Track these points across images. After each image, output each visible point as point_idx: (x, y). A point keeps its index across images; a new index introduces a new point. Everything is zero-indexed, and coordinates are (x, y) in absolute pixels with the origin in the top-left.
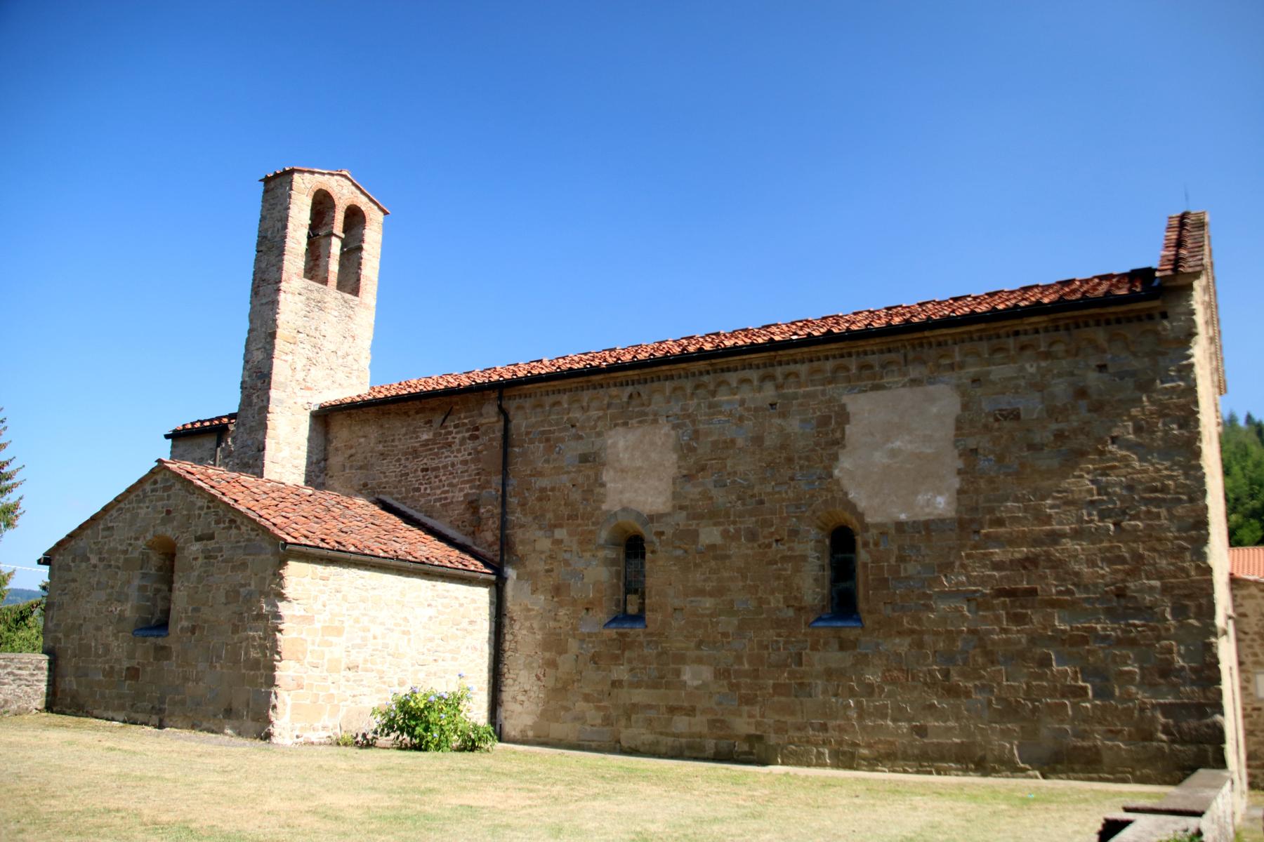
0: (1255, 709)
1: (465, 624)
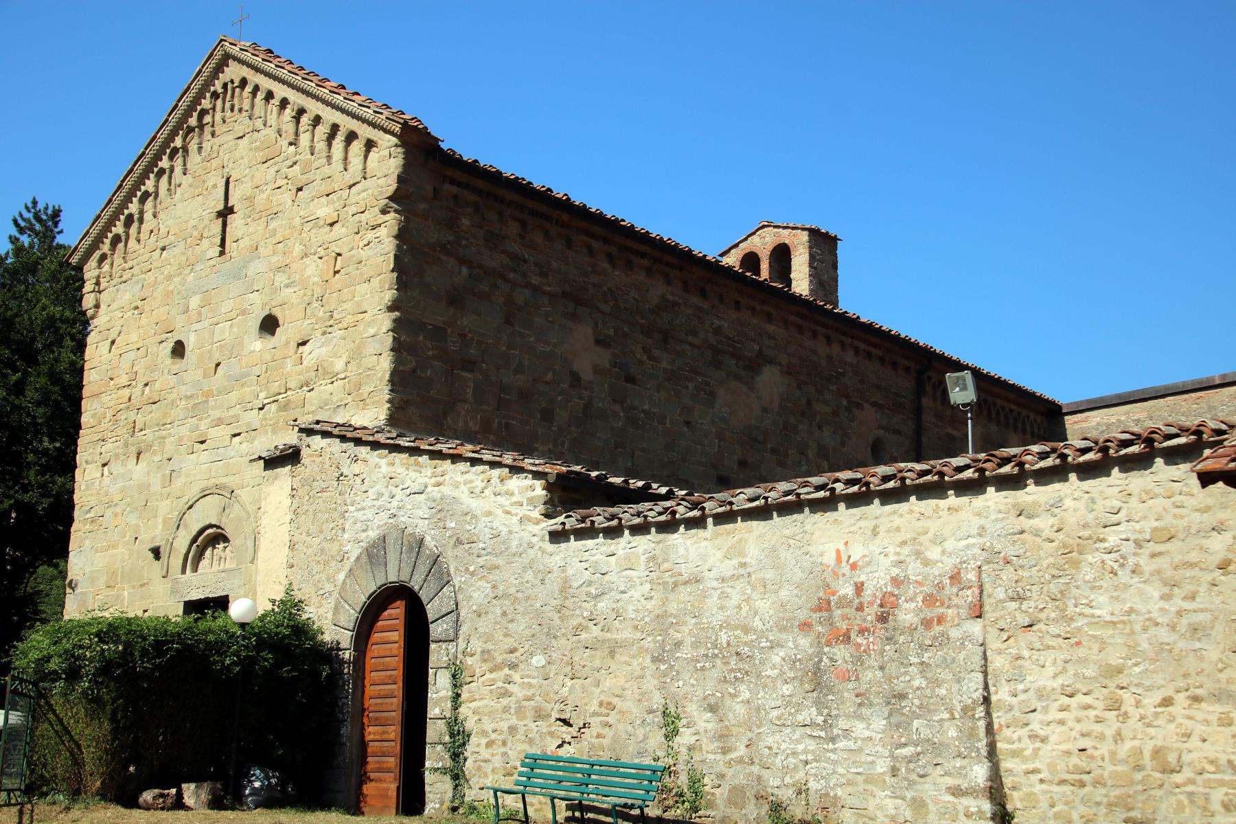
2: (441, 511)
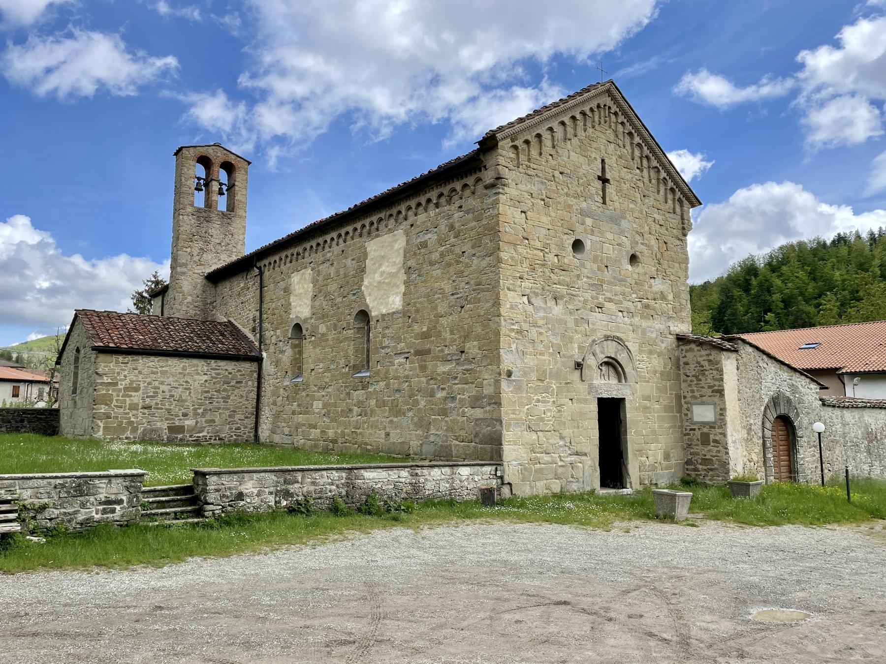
0: (691, 430)
1: (233, 383)
2: (794, 389)
